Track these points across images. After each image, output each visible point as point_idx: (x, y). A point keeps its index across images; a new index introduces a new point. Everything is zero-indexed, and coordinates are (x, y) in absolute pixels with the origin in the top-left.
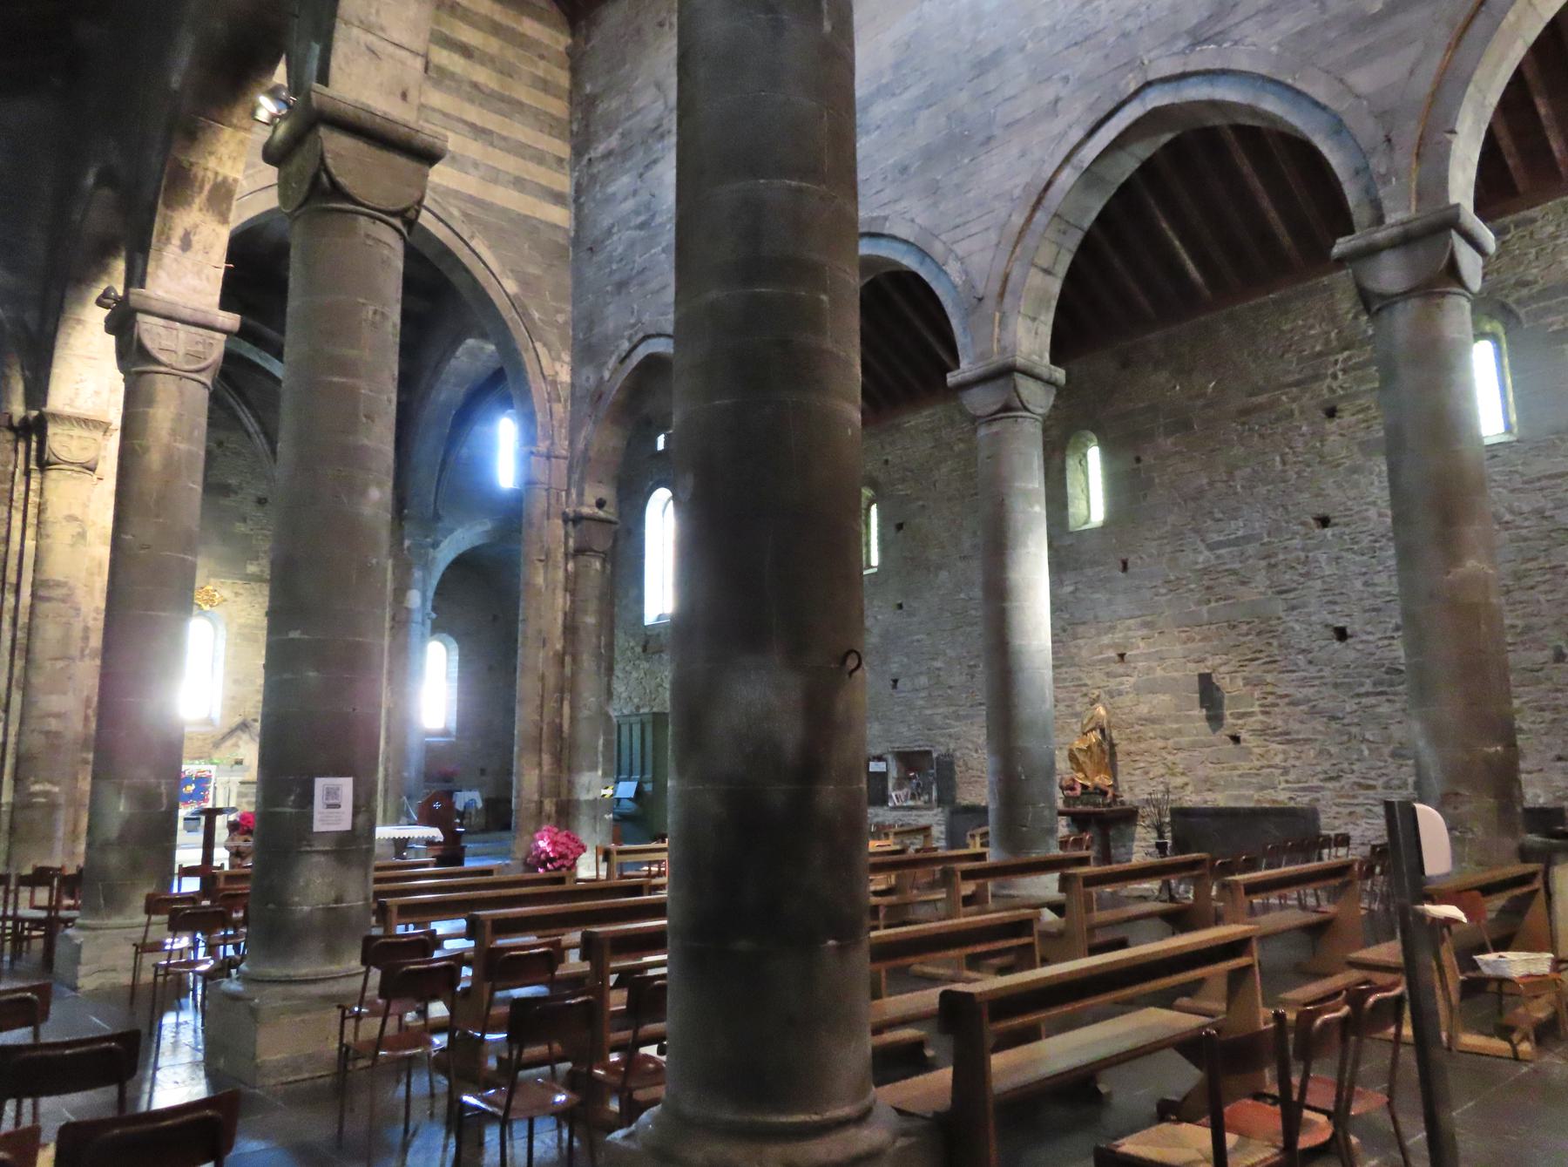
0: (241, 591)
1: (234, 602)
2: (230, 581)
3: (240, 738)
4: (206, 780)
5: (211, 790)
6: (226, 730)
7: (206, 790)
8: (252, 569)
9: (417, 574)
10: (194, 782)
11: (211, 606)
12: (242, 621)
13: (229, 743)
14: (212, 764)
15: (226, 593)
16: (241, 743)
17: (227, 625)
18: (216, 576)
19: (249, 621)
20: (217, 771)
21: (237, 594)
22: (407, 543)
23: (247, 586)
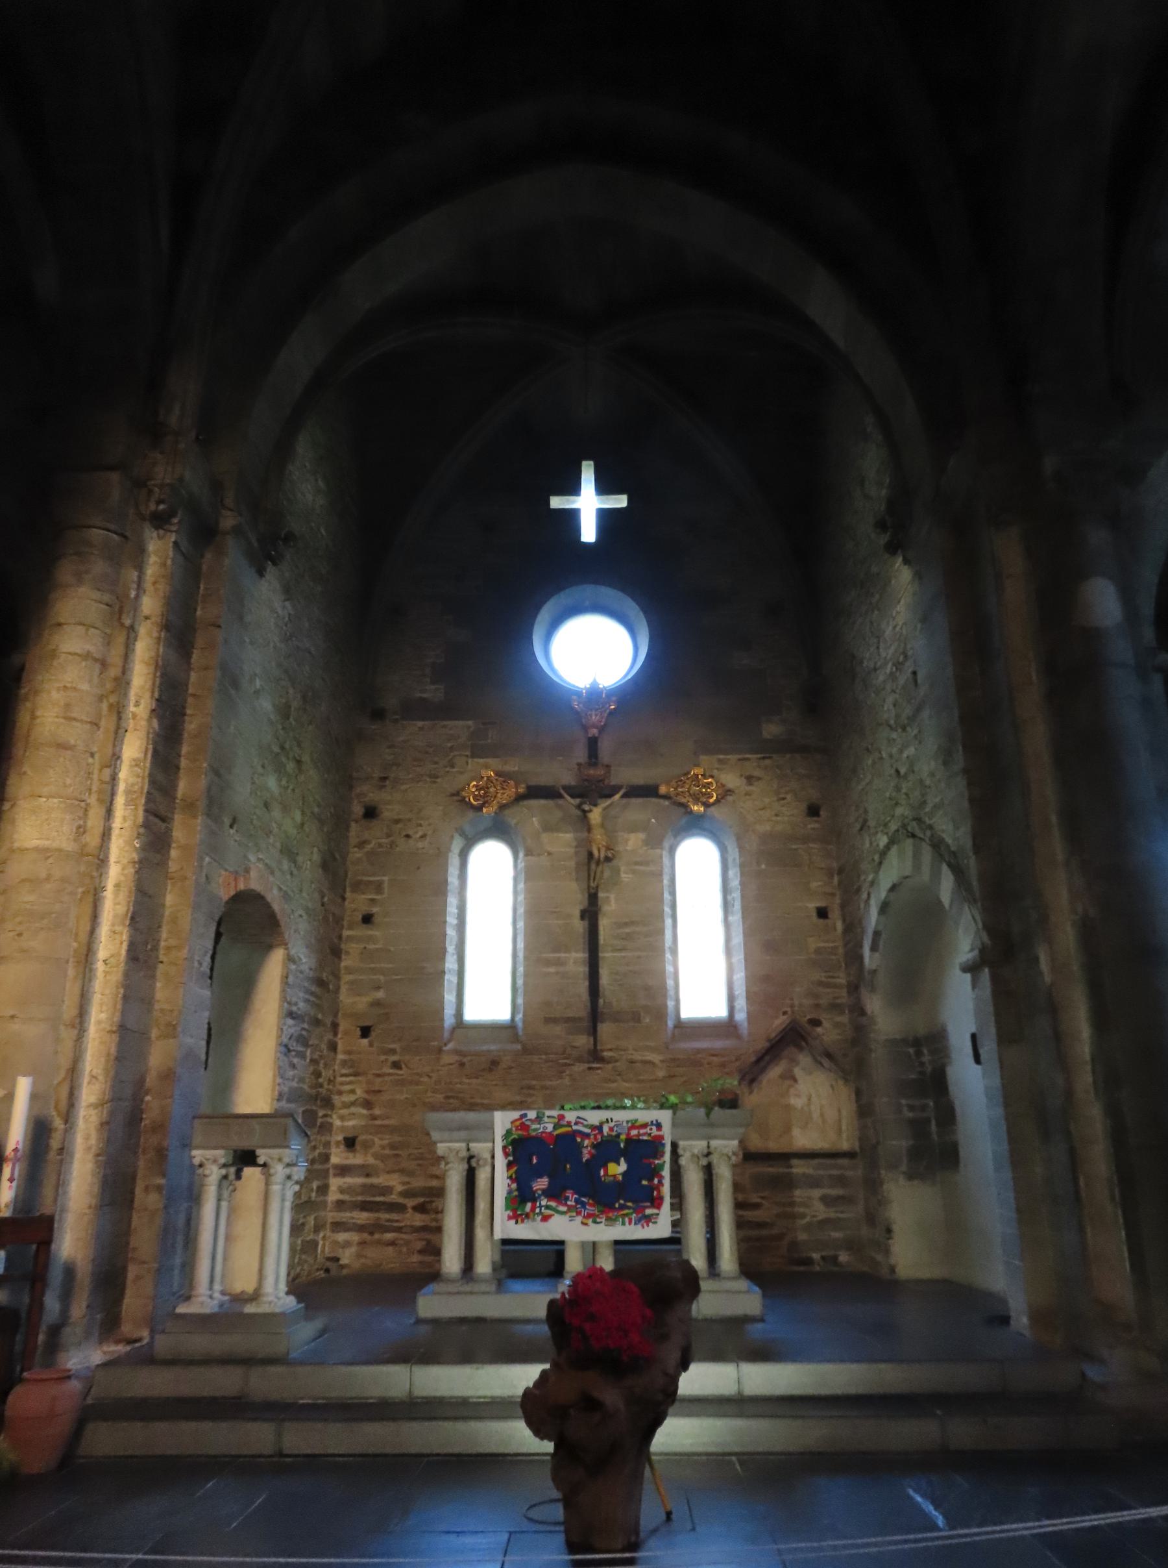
0: (757, 773)
1: (747, 794)
2: (733, 758)
3: (794, 1061)
4: (654, 1146)
5: (666, 1173)
6: (762, 1045)
7: (656, 1172)
8: (771, 730)
9: (1098, 537)
10: (625, 1153)
11: (707, 805)
12: (767, 827)
13: (774, 1072)
14: (662, 1107)
15: (731, 779)
16: (797, 1072)
17: (739, 839)
18: (708, 751)
19: (779, 828)
20: (674, 1125)
21: (750, 779)
22: (1049, 464)
23: (767, 762)
